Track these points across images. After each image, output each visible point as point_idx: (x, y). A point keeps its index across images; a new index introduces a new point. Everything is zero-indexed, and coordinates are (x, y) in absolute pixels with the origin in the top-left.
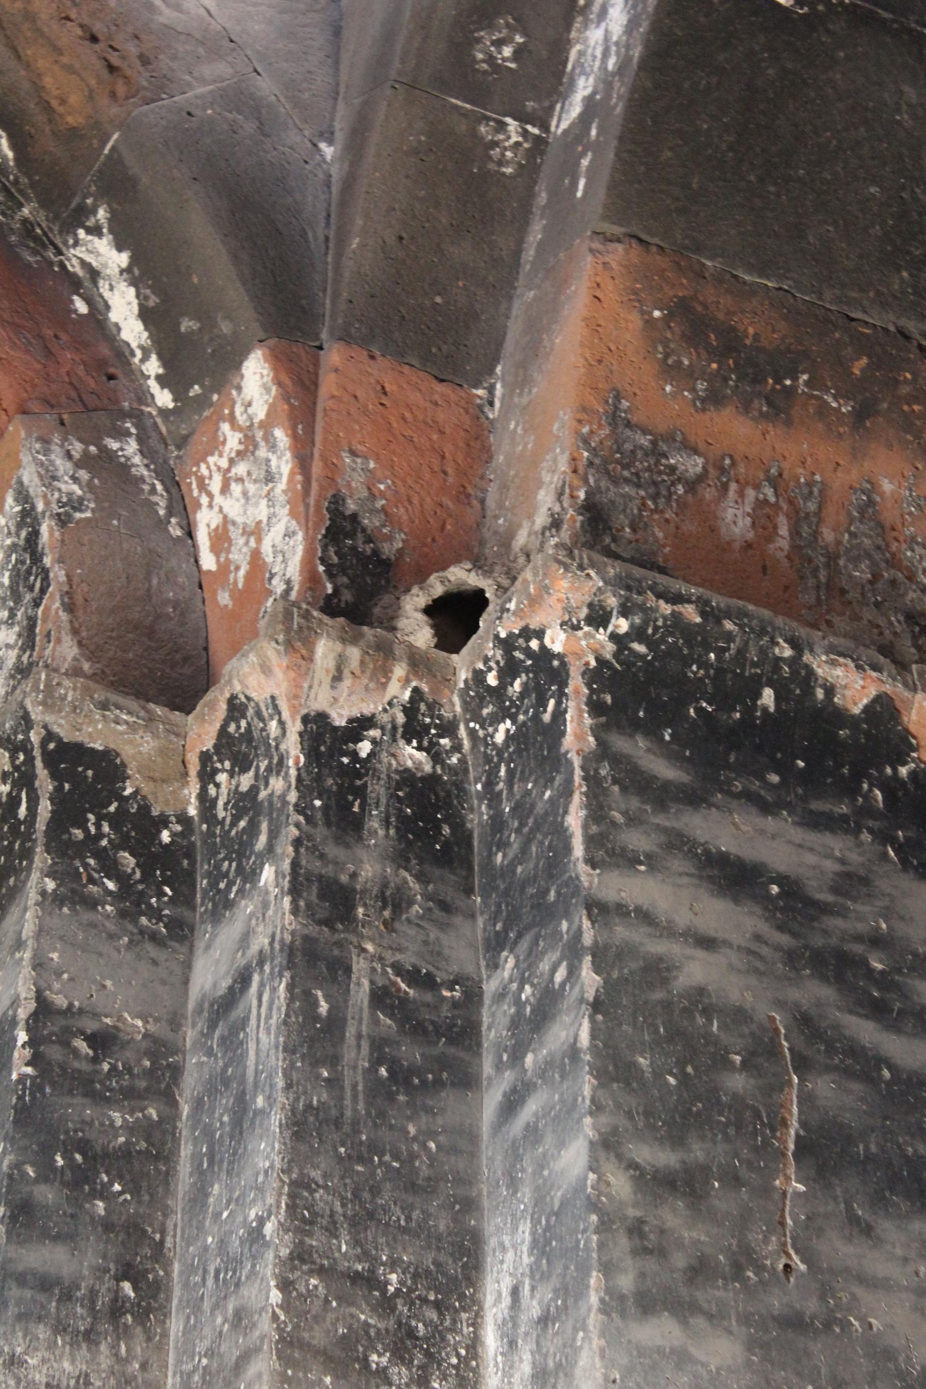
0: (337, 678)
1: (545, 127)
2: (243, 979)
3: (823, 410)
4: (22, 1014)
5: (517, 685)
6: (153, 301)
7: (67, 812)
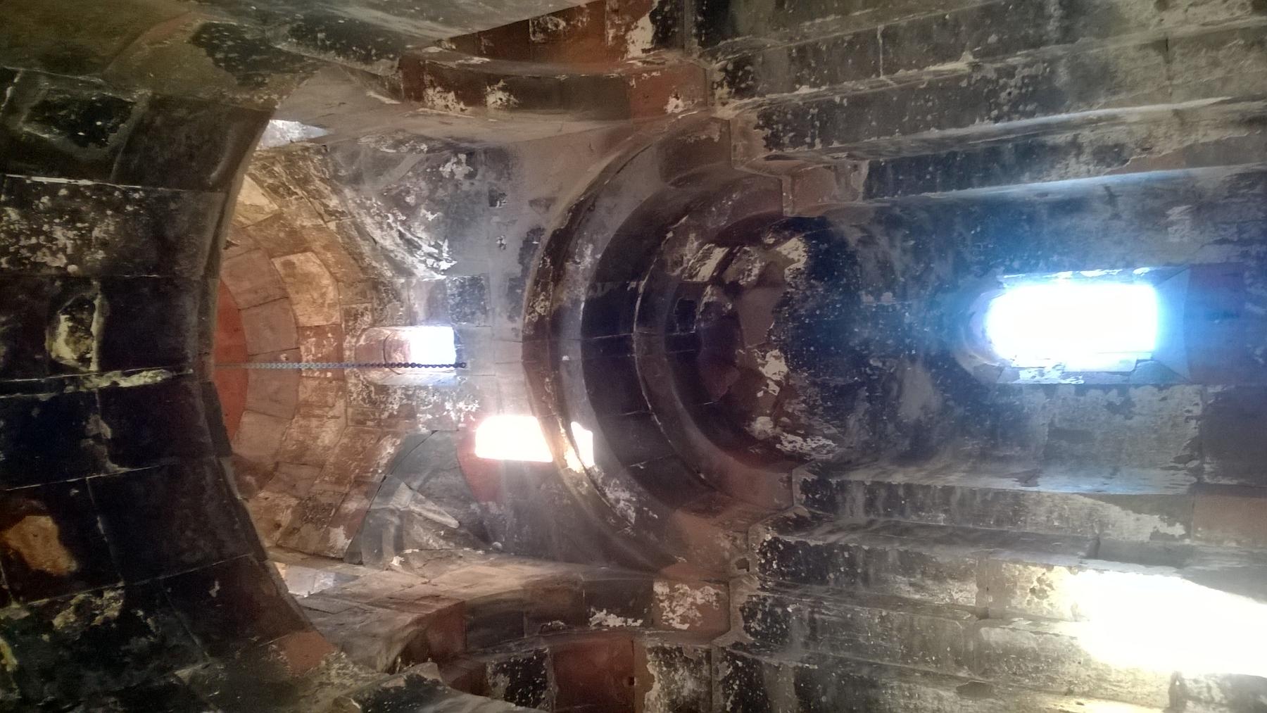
2: (813, 620)
6: (618, 610)
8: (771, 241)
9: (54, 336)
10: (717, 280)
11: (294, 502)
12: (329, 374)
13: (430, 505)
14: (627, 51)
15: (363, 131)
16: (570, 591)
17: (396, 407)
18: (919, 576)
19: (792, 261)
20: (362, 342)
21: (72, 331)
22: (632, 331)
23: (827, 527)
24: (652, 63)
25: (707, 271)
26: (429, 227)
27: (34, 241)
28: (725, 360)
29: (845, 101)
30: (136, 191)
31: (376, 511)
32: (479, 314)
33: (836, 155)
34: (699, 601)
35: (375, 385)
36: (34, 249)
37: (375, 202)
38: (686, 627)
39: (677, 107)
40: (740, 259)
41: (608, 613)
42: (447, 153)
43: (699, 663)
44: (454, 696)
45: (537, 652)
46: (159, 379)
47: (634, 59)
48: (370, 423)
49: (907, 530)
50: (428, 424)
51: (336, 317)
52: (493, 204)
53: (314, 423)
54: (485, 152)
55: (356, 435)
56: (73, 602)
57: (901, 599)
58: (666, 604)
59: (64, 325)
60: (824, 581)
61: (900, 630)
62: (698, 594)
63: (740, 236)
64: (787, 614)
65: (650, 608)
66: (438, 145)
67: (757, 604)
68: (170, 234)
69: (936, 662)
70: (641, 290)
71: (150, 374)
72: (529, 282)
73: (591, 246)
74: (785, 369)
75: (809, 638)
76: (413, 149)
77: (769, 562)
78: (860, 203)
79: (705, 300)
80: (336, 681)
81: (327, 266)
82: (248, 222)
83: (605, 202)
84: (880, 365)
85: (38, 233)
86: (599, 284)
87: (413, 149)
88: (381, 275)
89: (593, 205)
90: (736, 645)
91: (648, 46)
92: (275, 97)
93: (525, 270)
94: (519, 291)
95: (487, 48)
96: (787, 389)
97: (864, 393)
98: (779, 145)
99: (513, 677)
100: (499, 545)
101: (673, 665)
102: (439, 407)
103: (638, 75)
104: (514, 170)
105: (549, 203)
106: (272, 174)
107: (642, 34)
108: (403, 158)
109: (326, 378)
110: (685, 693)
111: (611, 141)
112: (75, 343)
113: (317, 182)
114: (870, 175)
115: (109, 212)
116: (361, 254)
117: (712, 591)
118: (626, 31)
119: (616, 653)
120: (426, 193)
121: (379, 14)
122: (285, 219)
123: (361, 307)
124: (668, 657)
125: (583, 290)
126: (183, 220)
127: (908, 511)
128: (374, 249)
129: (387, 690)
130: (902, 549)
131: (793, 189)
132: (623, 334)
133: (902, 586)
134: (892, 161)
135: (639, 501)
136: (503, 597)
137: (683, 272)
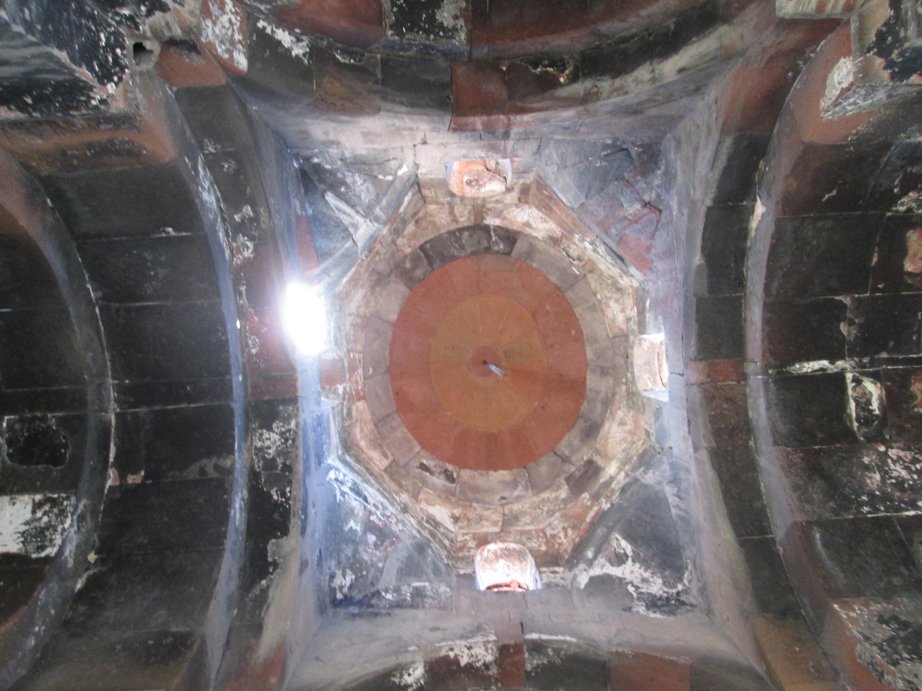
0: (168, 24)
1: (204, 154)
3: (76, 149)
5: (110, 59)
9: (880, 398)
11: (400, 241)
13: (346, 220)
21: (869, 402)
22: (117, 415)
26: (351, 513)
30: (869, 512)
37: (396, 528)
41: (289, 50)
42: (357, 596)
45: (401, 35)
46: (797, 366)
51: (354, 408)
52: (320, 551)
53: (362, 310)
59: (875, 406)
66: (374, 601)
68: (819, 482)
71: (805, 370)
72: (300, 467)
77: (110, 47)
82: (426, 490)
87: (397, 590)
88: (350, 456)
99: (432, 18)
108: (399, 579)
112: (865, 393)
120: (361, 548)
126: (817, 496)
132: (142, 410)
136: (403, 109)
137: (76, 507)
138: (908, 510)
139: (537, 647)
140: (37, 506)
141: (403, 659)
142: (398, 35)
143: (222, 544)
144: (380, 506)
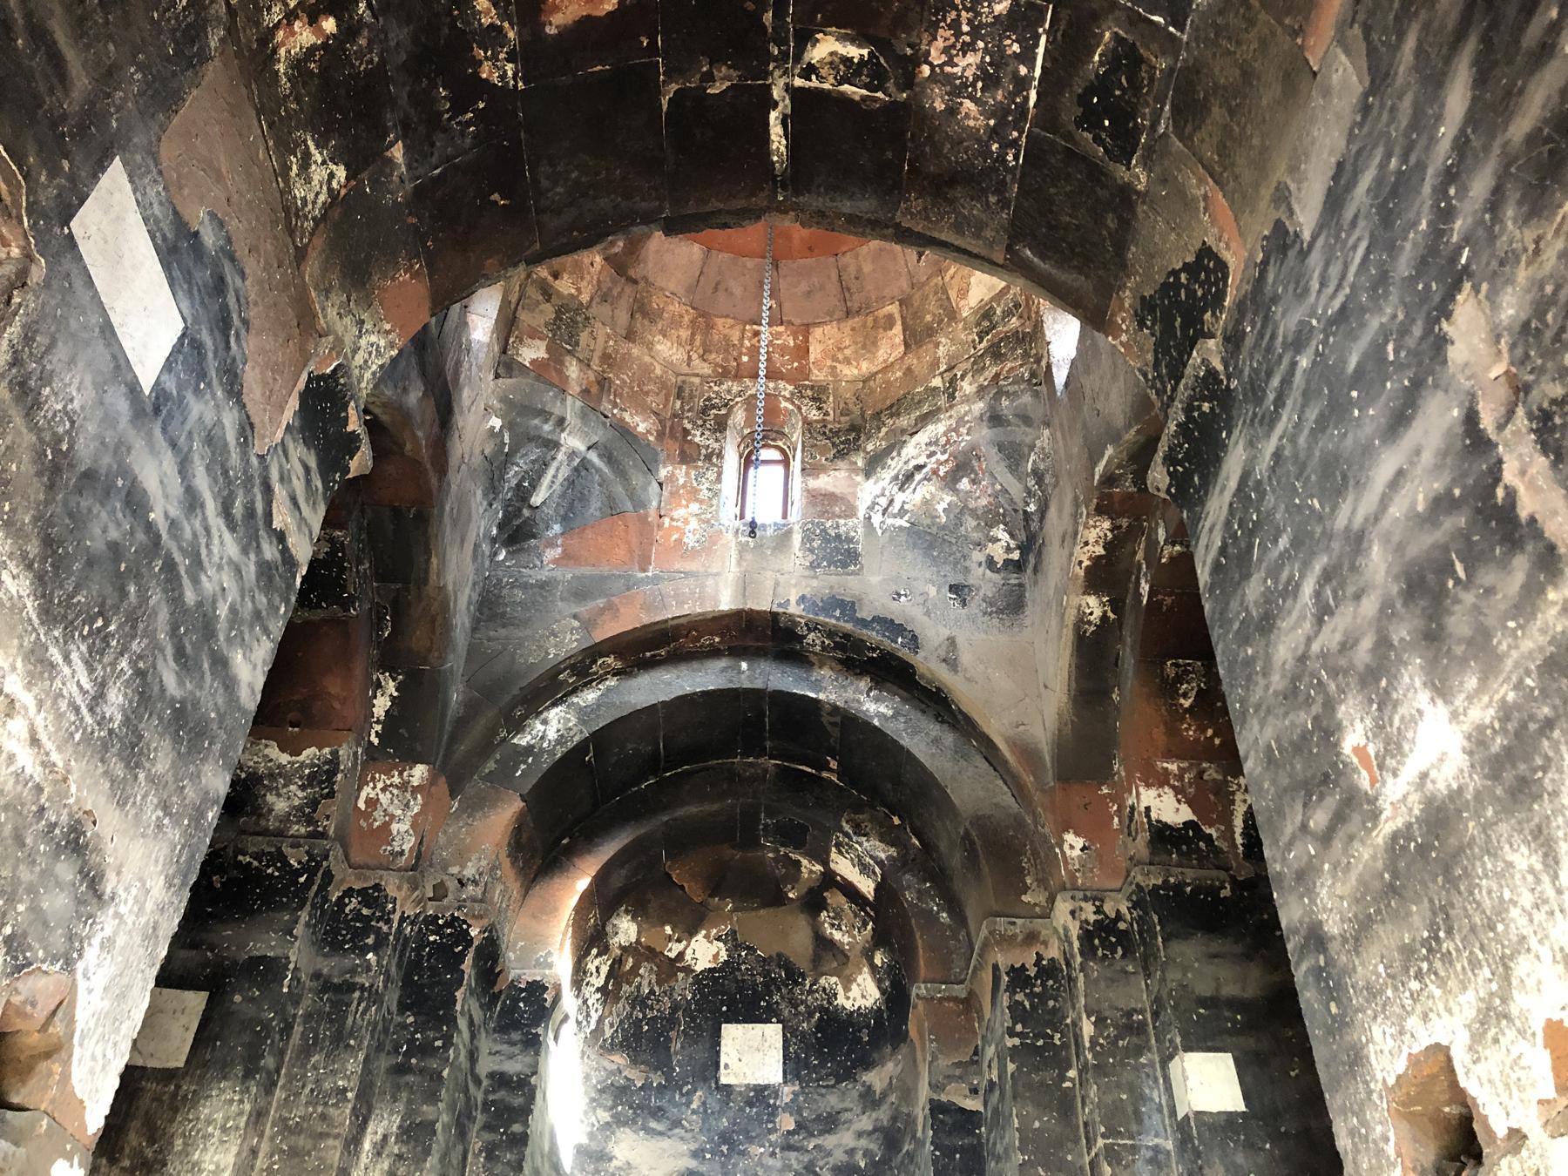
2: (352, 987)
4: (291, 966)
7: (316, 895)
8: (878, 961)
9: (841, 38)
10: (830, 880)
11: (585, 298)
12: (745, 359)
13: (565, 472)
14: (1148, 786)
15: (1059, 434)
16: (430, 650)
17: (697, 439)
18: (396, 1151)
19: (847, 989)
20: (784, 404)
21: (847, 60)
23: (478, 1015)
24: (1131, 819)
25: (844, 867)
27: (965, 28)
28: (718, 885)
29: (1067, 1084)
30: (1016, 158)
31: (564, 400)
32: (812, 557)
33: (995, 1065)
34: (395, 827)
35: (727, 416)
36: (955, 26)
37: (965, 440)
38: (361, 805)
39: (1072, 847)
40: (856, 916)
41: (393, 698)
42: (1022, 536)
43: (310, 821)
44: (324, 494)
47: (1138, 794)
48: (678, 403)
49: (462, 1134)
50: (671, 478)
51: (818, 375)
52: (952, 588)
53: (685, 334)
54: (1021, 585)
55: (663, 384)
56: (506, 25)
57: (366, 1121)
58: (396, 780)
59: (855, 52)
60: (403, 1008)
61: (323, 1117)
62: (404, 826)
63: (887, 918)
64: (364, 950)
65: (393, 757)
66: (1034, 526)
67: (383, 911)
68: (958, 192)
69: (269, 1169)
70: (825, 775)
71: (782, 149)
73: (890, 713)
74: (699, 968)
75: (326, 982)
76: (1029, 493)
77: (439, 930)
78: (924, 1093)
79: (805, 862)
80: (363, 342)
81: (885, 370)
82: (947, 278)
83: (949, 738)
84: (694, 1106)
85: (975, 33)
86: (838, 719)
87: (1029, 493)
89: (942, 722)
90: (328, 877)
91: (1154, 815)
92: (1124, 338)
93: (863, 623)
94: (837, 613)
95: (1160, 603)
96: (671, 968)
97: (657, 1079)
98: (1012, 989)
100: (501, 557)
101: (311, 785)
102: (694, 494)
103: (1118, 798)
104: (996, 621)
105: (952, 663)
106: (1008, 314)
107: (1168, 808)
108: (1020, 480)
109: (741, 354)
110: (270, 798)
111: (1028, 753)
112: (831, 63)
113: (995, 370)
114: (962, 1110)
115: (992, 122)
116: (898, 415)
117: (406, 847)
118: (1173, 787)
119: (337, 705)
121: (1233, 484)
122: (949, 325)
123: (829, 407)
124: (323, 779)
125: (833, 697)
127: (488, 1136)
128: (903, 431)
129: (345, 407)
130: (438, 1126)
131: (949, 999)
132: (768, 744)
133: (385, 1122)
134: (980, 1144)
135: (542, 750)
136: (434, 560)
137: (846, 835)
138: (1027, 99)
139: (1109, 480)
140: (840, 853)
141: (1071, 617)
142: (353, 603)
143: (902, 747)
144: (932, 449)
